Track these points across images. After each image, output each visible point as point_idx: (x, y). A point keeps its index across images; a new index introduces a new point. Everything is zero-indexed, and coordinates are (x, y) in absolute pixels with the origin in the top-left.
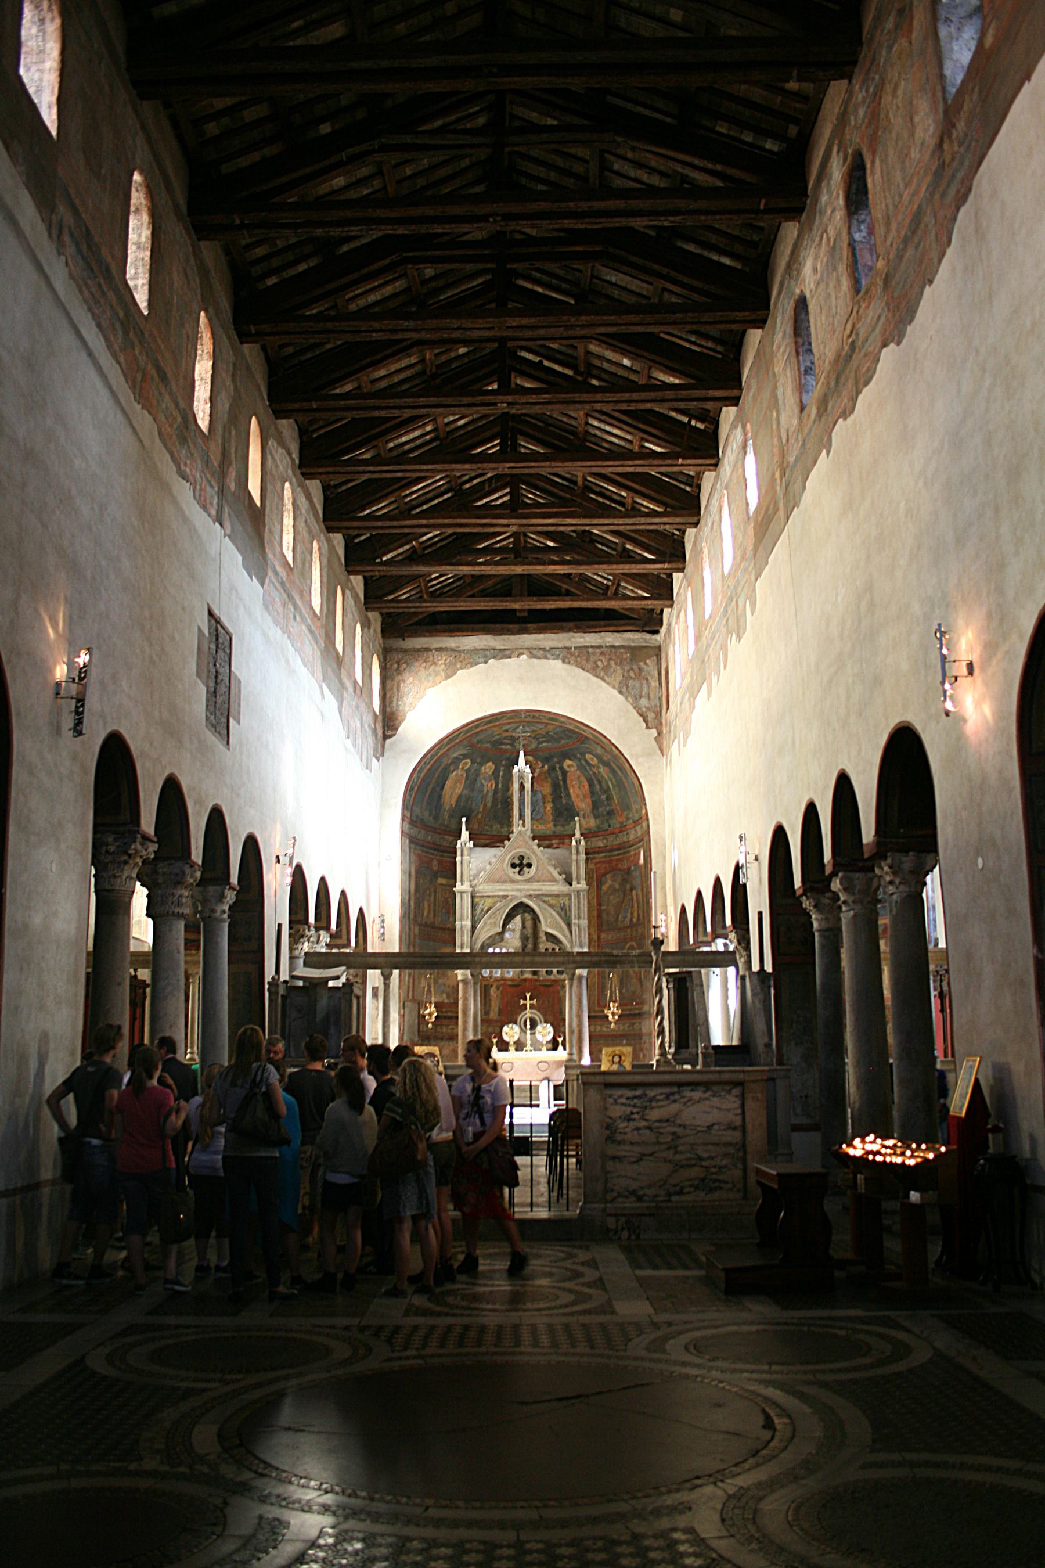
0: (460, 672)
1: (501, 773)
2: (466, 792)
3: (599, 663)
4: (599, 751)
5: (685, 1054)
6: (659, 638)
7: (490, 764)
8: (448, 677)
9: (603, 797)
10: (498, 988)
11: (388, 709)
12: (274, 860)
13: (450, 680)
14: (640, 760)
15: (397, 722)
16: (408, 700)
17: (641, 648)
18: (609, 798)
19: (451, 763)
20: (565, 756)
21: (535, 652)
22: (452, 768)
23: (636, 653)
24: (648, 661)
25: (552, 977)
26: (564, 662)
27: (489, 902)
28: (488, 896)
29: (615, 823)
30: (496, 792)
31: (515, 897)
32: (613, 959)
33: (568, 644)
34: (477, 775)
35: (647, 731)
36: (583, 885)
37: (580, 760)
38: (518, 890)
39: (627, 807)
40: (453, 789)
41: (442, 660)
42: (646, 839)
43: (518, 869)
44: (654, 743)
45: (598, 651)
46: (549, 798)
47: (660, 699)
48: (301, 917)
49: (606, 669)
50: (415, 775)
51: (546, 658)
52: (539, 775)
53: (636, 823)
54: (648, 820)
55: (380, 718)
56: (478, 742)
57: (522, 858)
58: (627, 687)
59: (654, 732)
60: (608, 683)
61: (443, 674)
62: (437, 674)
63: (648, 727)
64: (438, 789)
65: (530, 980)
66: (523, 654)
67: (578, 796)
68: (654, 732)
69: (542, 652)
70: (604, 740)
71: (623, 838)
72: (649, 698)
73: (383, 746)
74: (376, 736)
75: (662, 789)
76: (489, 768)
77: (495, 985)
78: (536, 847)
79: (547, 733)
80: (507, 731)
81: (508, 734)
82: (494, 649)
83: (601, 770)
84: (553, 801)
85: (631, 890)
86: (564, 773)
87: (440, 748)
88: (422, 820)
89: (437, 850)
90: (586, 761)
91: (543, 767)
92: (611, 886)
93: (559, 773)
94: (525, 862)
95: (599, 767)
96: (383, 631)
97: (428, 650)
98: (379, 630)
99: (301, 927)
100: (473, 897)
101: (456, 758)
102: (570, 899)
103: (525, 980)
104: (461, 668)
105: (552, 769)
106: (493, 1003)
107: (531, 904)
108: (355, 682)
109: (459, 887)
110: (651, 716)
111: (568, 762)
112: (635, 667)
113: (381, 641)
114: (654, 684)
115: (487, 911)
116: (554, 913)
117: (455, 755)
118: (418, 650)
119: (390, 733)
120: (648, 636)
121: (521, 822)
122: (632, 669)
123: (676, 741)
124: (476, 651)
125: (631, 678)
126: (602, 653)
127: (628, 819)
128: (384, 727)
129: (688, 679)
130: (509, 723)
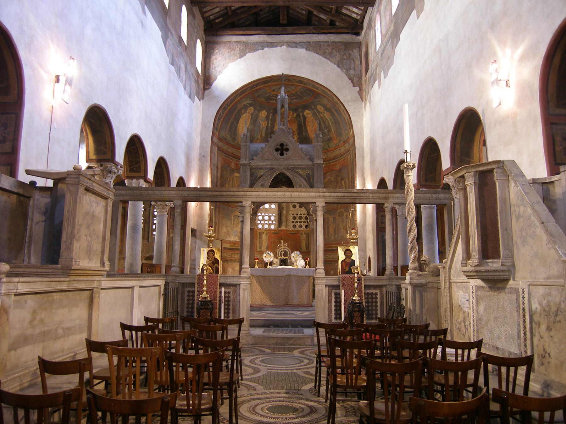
0: (248, 55)
1: (270, 117)
2: (250, 127)
3: (327, 51)
4: (325, 102)
5: (494, 265)
6: (361, 38)
7: (264, 111)
8: (241, 57)
9: (326, 131)
10: (266, 234)
11: (207, 74)
12: (54, 79)
13: (242, 59)
14: (350, 103)
15: (212, 81)
16: (218, 69)
17: (350, 43)
18: (329, 131)
19: (243, 108)
20: (306, 107)
21: (290, 44)
22: (243, 111)
23: (348, 46)
24: (354, 50)
25: (296, 229)
26: (306, 50)
27: (261, 172)
28: (261, 168)
29: (332, 145)
30: (267, 128)
31: (278, 169)
32: (353, 195)
33: (309, 40)
34: (257, 118)
35: (354, 88)
36: (320, 162)
37: (313, 110)
38: (279, 165)
39: (339, 134)
40: (243, 127)
41: (238, 48)
42: (351, 150)
43: (279, 152)
44: (357, 94)
45: (326, 44)
46: (296, 133)
47: (361, 71)
48: (108, 156)
49: (330, 54)
50: (221, 111)
51: (297, 47)
52: (291, 119)
53: (345, 142)
54: (354, 137)
55: (202, 78)
56: (258, 96)
57: (282, 145)
58: (342, 64)
59: (357, 89)
60: (332, 62)
61: (238, 55)
62: (235, 55)
63: (354, 86)
64: (235, 123)
65: (284, 230)
66: (284, 45)
67: (312, 131)
68: (357, 89)
69: (294, 44)
70: (328, 92)
71: (337, 152)
72: (355, 70)
73: (203, 94)
74: (199, 86)
75: (362, 120)
76: (263, 114)
77: (265, 233)
78: (291, 139)
79: (296, 93)
80: (274, 90)
81: (275, 93)
82: (267, 42)
83: (326, 115)
84: (298, 134)
85: (341, 180)
86: (305, 118)
87: (236, 97)
88: (226, 139)
89: (234, 157)
90: (317, 110)
91: (293, 114)
92: (329, 179)
93: (302, 118)
94: (284, 148)
95: (324, 113)
96: (205, 31)
97: (230, 42)
98: (202, 28)
99: (109, 165)
100: (251, 169)
101: (245, 105)
102: (313, 171)
103: (281, 230)
104: (249, 52)
105: (298, 116)
106: (264, 243)
107: (288, 174)
108: (180, 38)
109: (243, 161)
110: (356, 79)
111: (307, 111)
112: (347, 53)
113: (204, 37)
114: (358, 62)
115: (260, 178)
116: (302, 179)
117: (245, 103)
118: (225, 43)
119: (207, 87)
120: (354, 37)
121: (282, 123)
122: (345, 54)
123: (377, 83)
124: (257, 43)
125: (345, 59)
126: (328, 45)
127: (340, 141)
128: (204, 84)
129: (392, 28)
130: (276, 85)
